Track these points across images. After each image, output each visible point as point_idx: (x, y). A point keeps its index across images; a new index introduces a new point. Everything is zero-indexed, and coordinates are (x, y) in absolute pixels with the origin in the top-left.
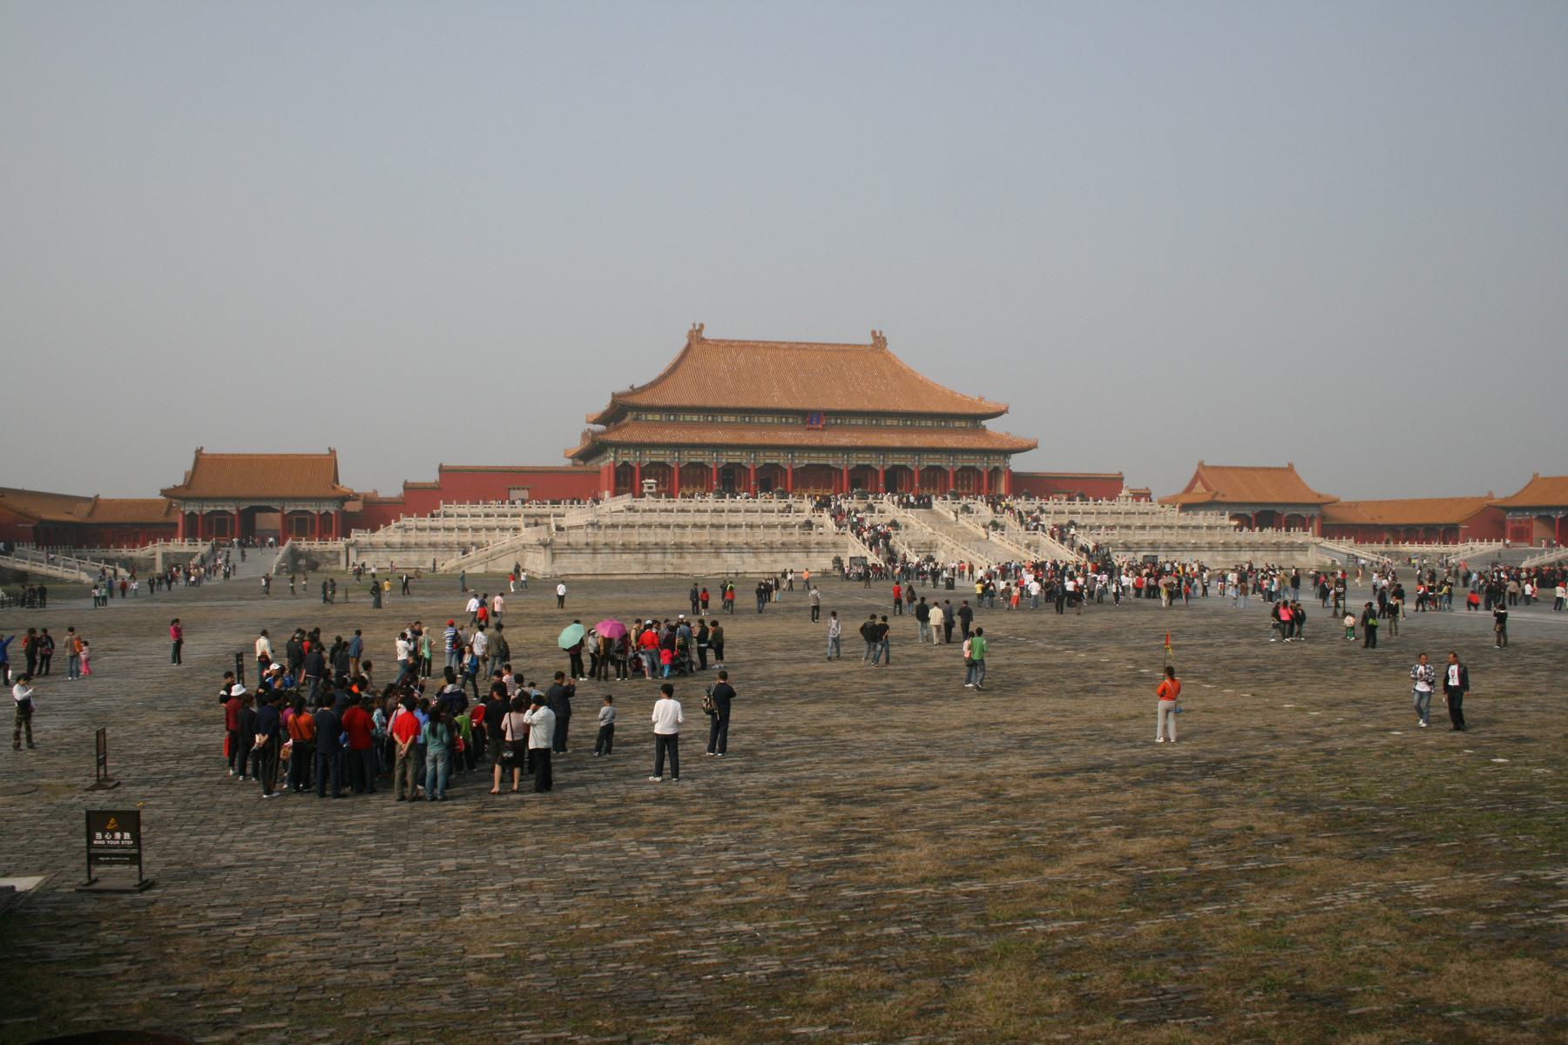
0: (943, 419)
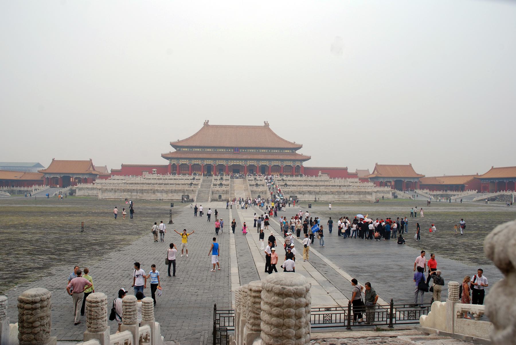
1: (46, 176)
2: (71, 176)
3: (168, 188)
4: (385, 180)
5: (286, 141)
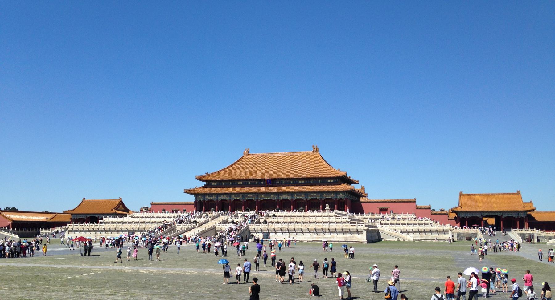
2: (96, 216)
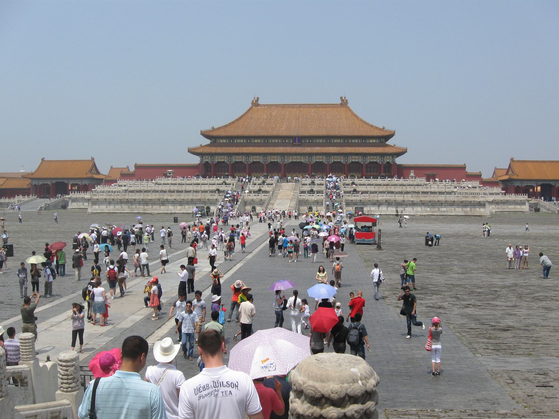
0: (363, 140)
1: (34, 183)
2: (66, 181)
3: (182, 197)
4: (525, 184)
5: (372, 126)
